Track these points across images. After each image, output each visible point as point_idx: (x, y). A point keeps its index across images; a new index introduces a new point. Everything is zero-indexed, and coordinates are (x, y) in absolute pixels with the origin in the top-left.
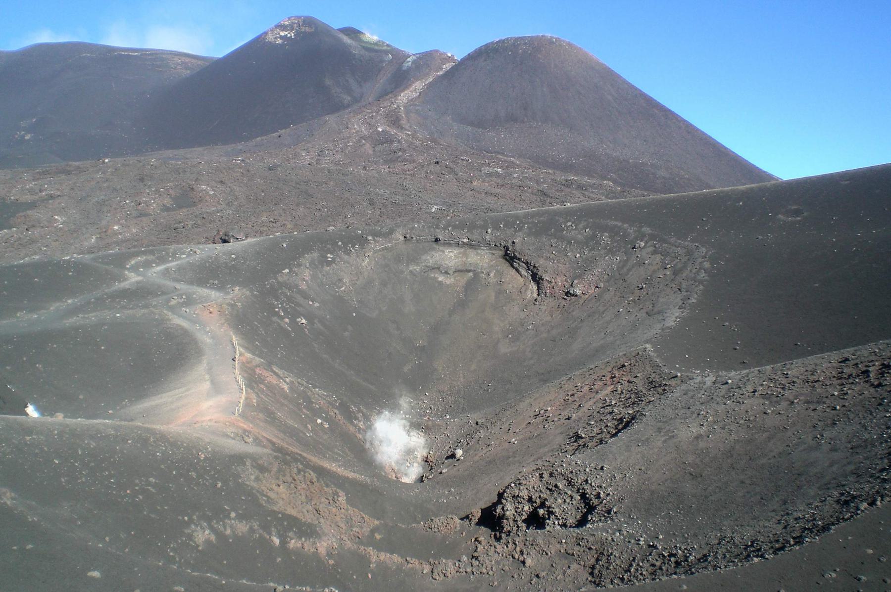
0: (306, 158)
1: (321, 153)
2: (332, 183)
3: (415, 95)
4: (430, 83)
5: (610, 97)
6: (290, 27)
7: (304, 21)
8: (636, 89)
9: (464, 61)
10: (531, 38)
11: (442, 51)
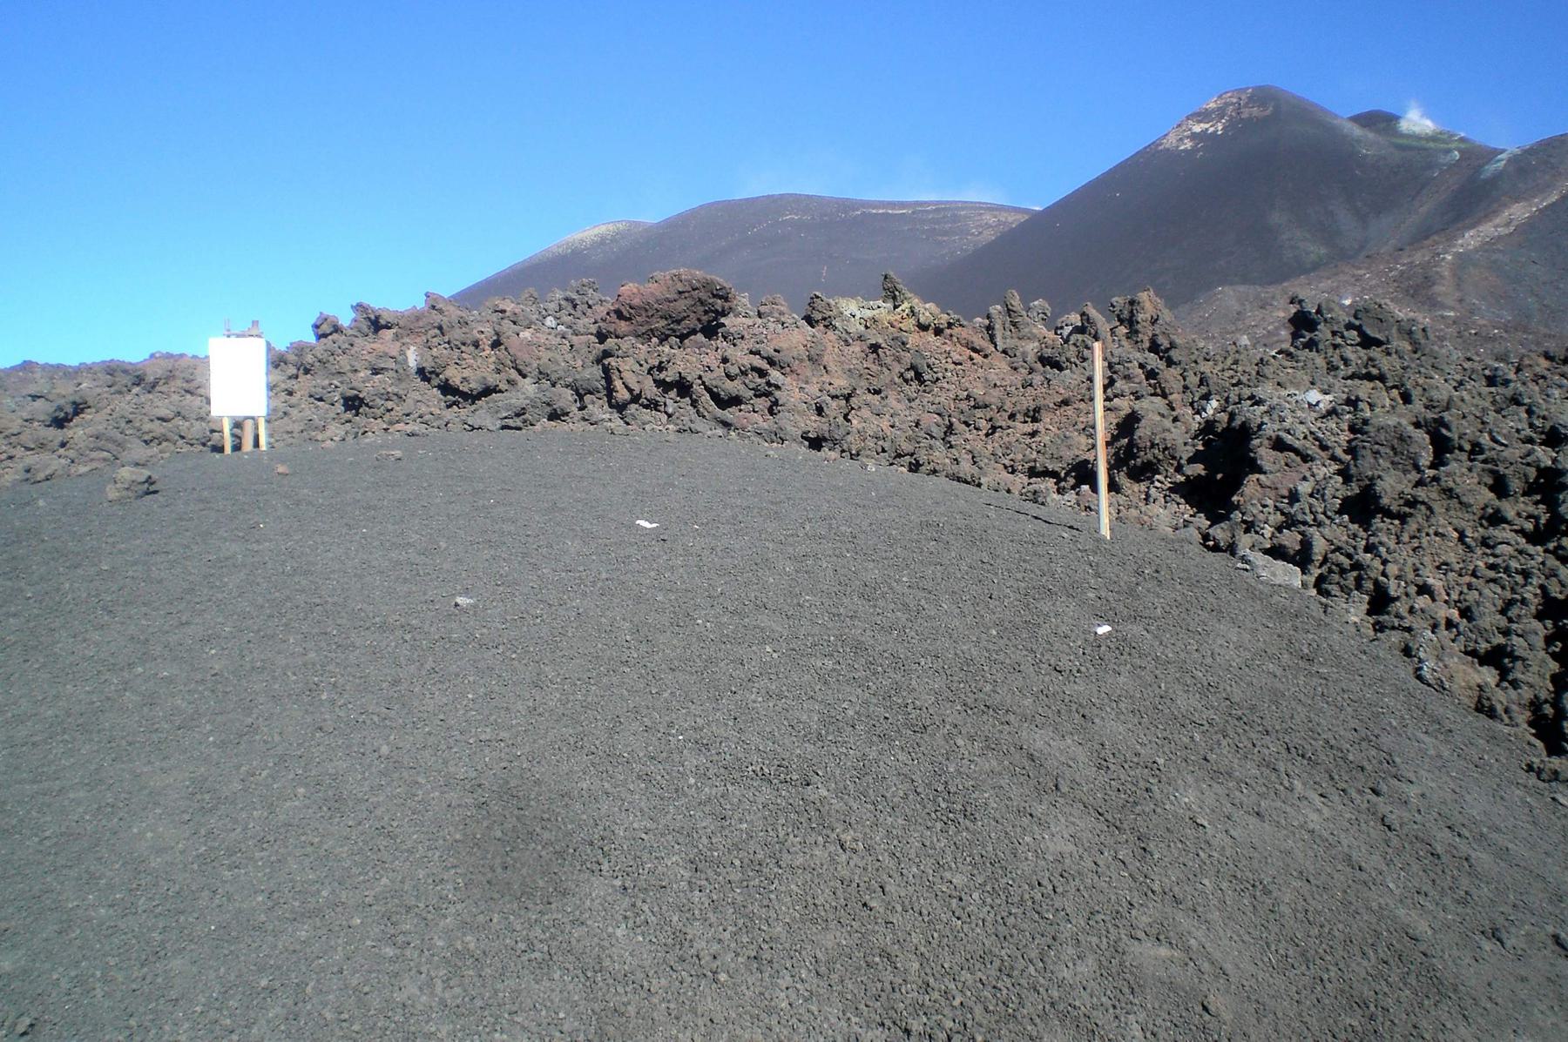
6: (1220, 112)
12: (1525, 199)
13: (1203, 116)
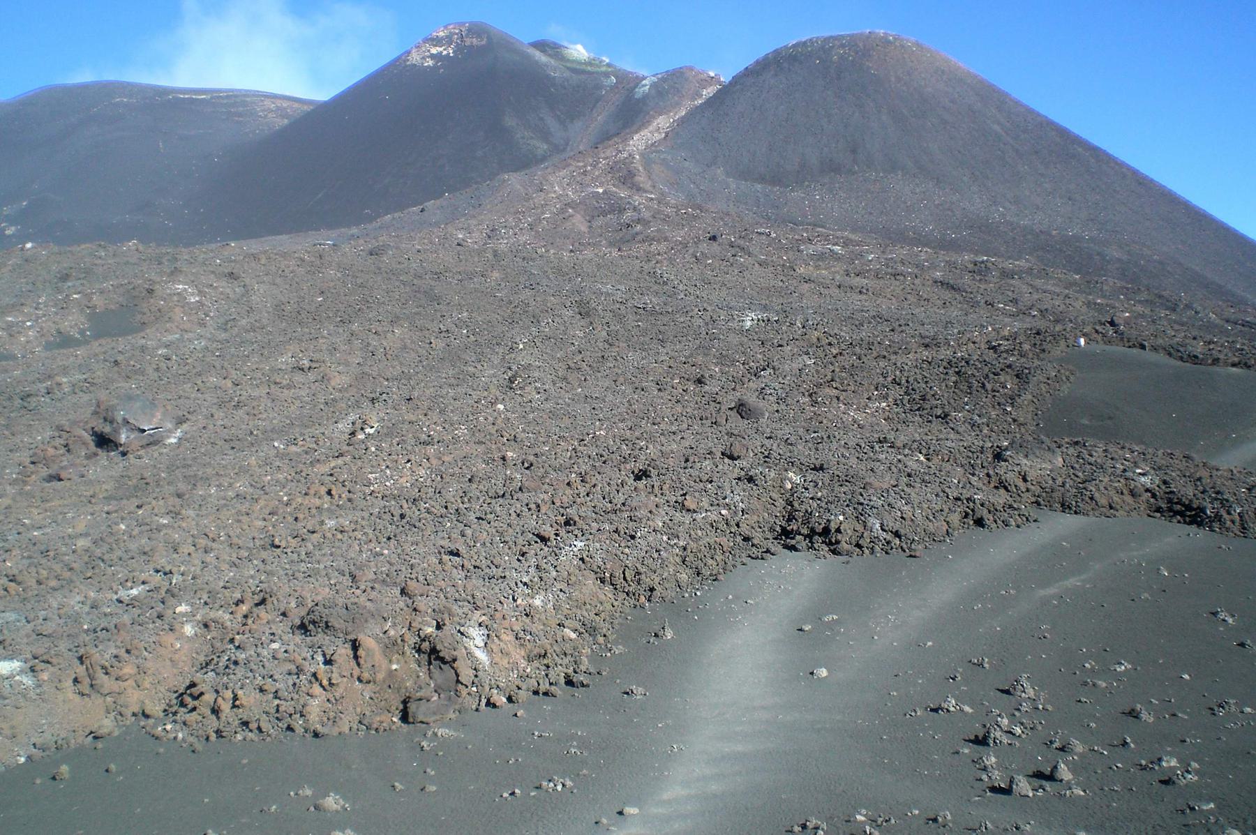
1: (492, 233)
2: (496, 275)
3: (657, 137)
4: (683, 117)
5: (996, 127)
6: (448, 40)
7: (469, 30)
8: (1038, 114)
9: (736, 80)
10: (851, 36)
11: (698, 68)
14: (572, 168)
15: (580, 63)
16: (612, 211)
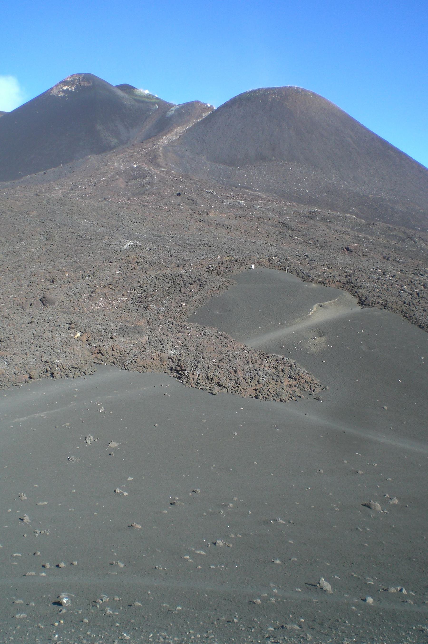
0: (58, 191)
3: (175, 138)
6: (72, 83)
7: (84, 78)
8: (373, 133)
10: (280, 88)
11: (202, 101)
12: (181, 126)
13: (64, 83)
14: (126, 153)
15: (142, 97)
16: (140, 177)
